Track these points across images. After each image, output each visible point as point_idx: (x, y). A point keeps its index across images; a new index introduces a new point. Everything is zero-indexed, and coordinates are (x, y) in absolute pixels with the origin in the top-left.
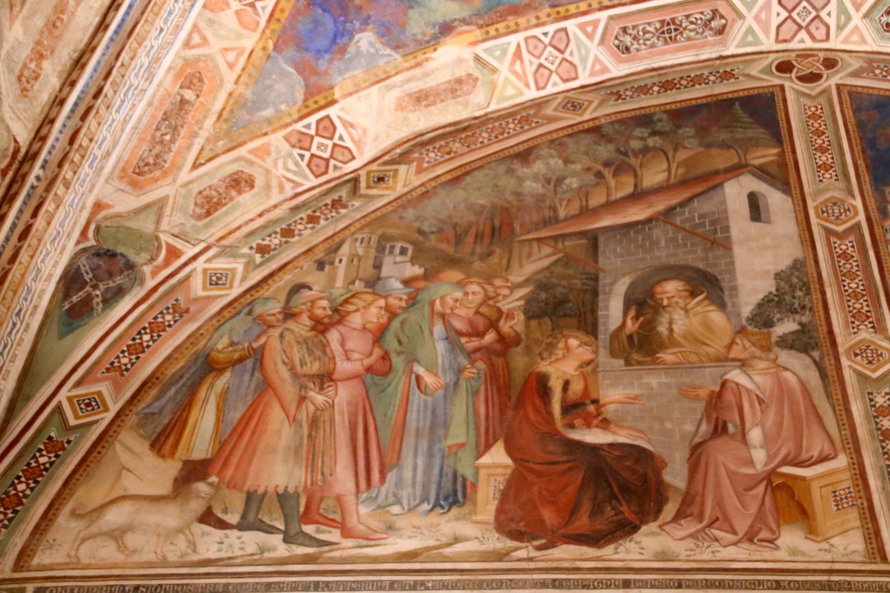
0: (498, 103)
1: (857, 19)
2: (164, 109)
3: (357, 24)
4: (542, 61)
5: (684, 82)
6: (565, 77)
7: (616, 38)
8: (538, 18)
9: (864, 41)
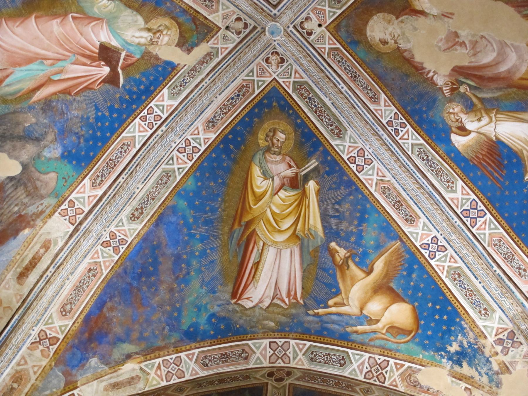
0: (148, 388)
1: (300, 356)
2: (4, 391)
3: (91, 355)
4: (169, 370)
5: (229, 380)
6: (179, 376)
7: (202, 360)
8: (168, 352)
9: (303, 365)
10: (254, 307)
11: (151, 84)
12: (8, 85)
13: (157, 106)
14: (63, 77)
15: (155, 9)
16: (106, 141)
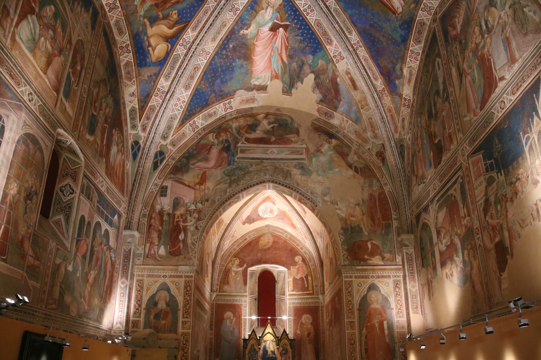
10: (402, 8)
11: (292, 9)
12: (278, 71)
13: (304, 7)
14: (280, 48)
15: (258, 5)
16: (313, 33)
